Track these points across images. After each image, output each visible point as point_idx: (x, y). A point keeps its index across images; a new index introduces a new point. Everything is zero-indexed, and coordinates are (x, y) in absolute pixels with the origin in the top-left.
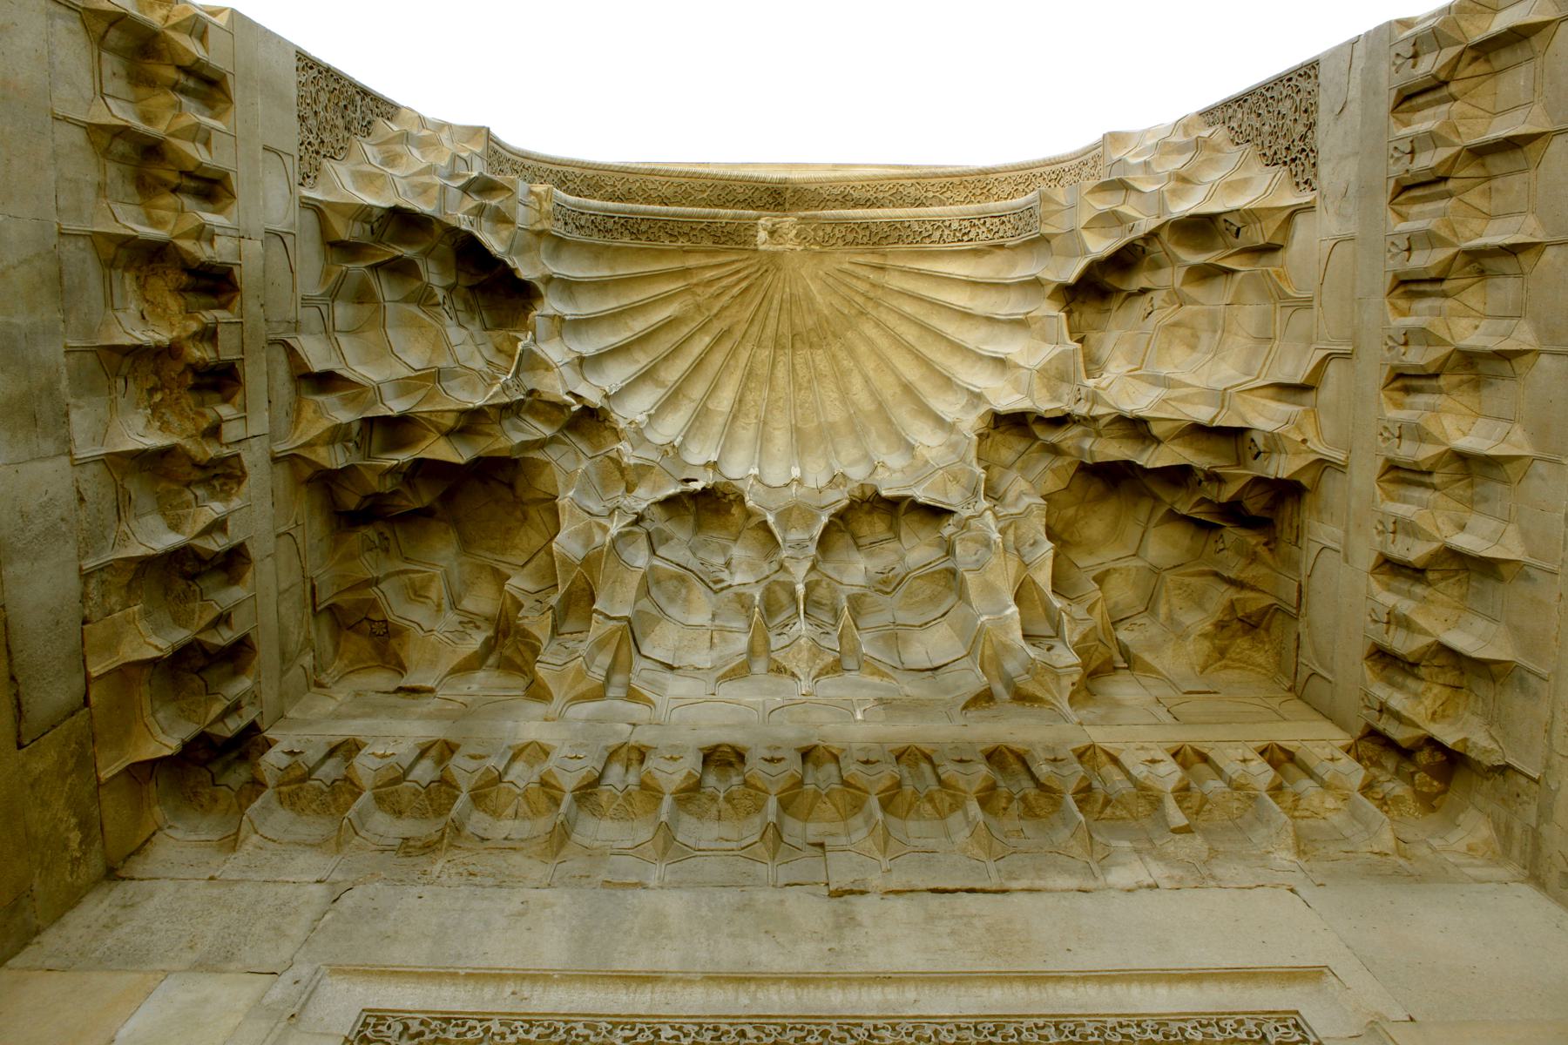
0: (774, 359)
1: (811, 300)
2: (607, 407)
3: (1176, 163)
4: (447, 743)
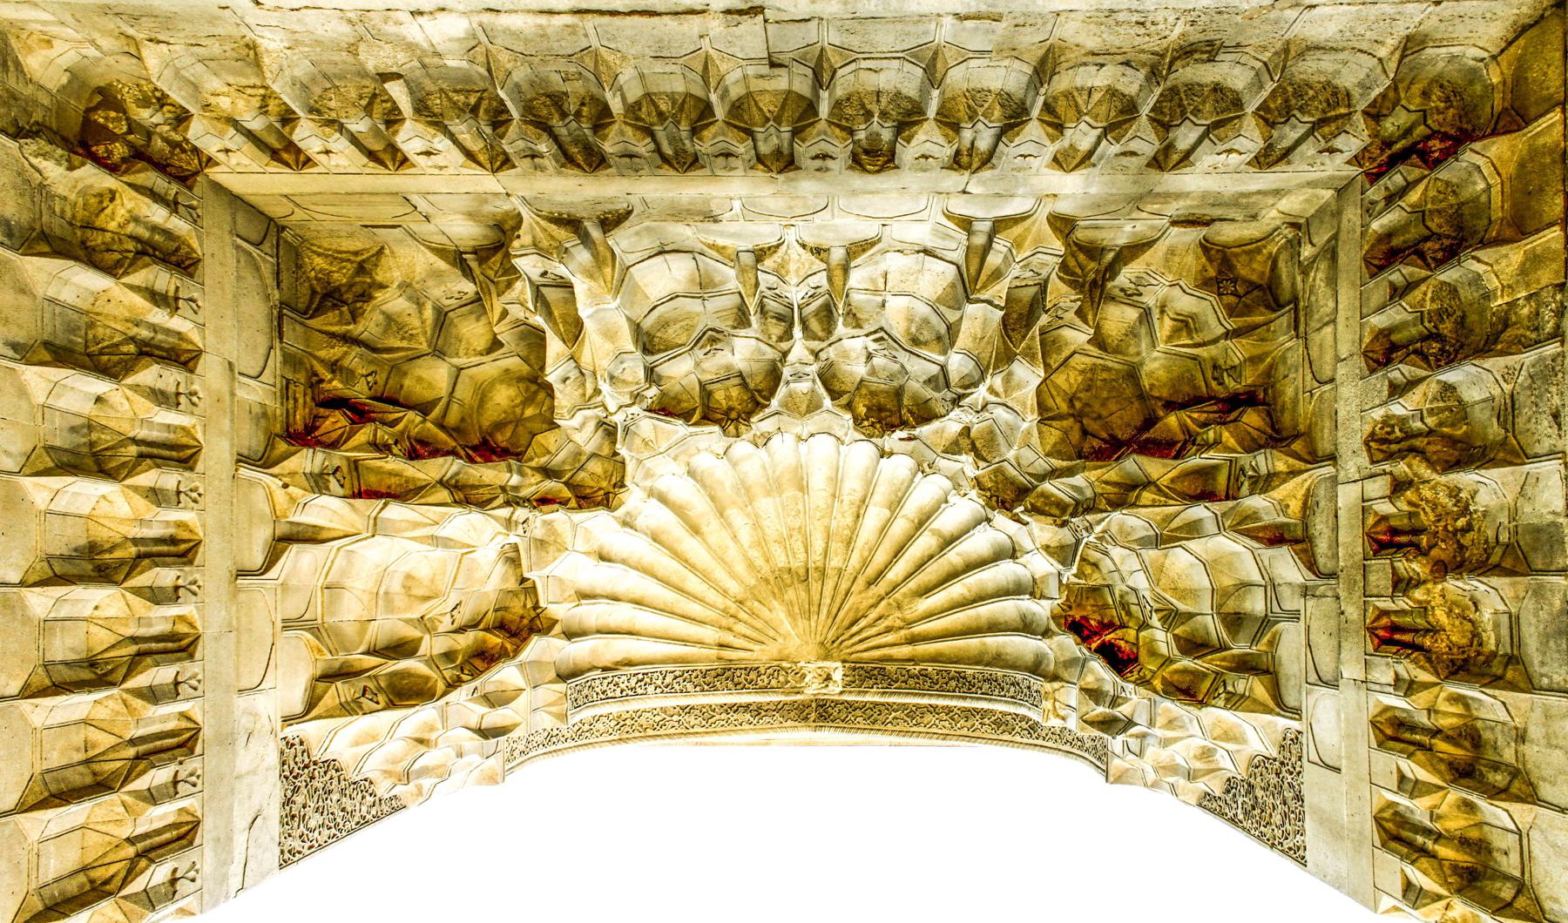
0: (825, 557)
1: (790, 614)
2: (988, 510)
3: (431, 758)
4: (1161, 169)
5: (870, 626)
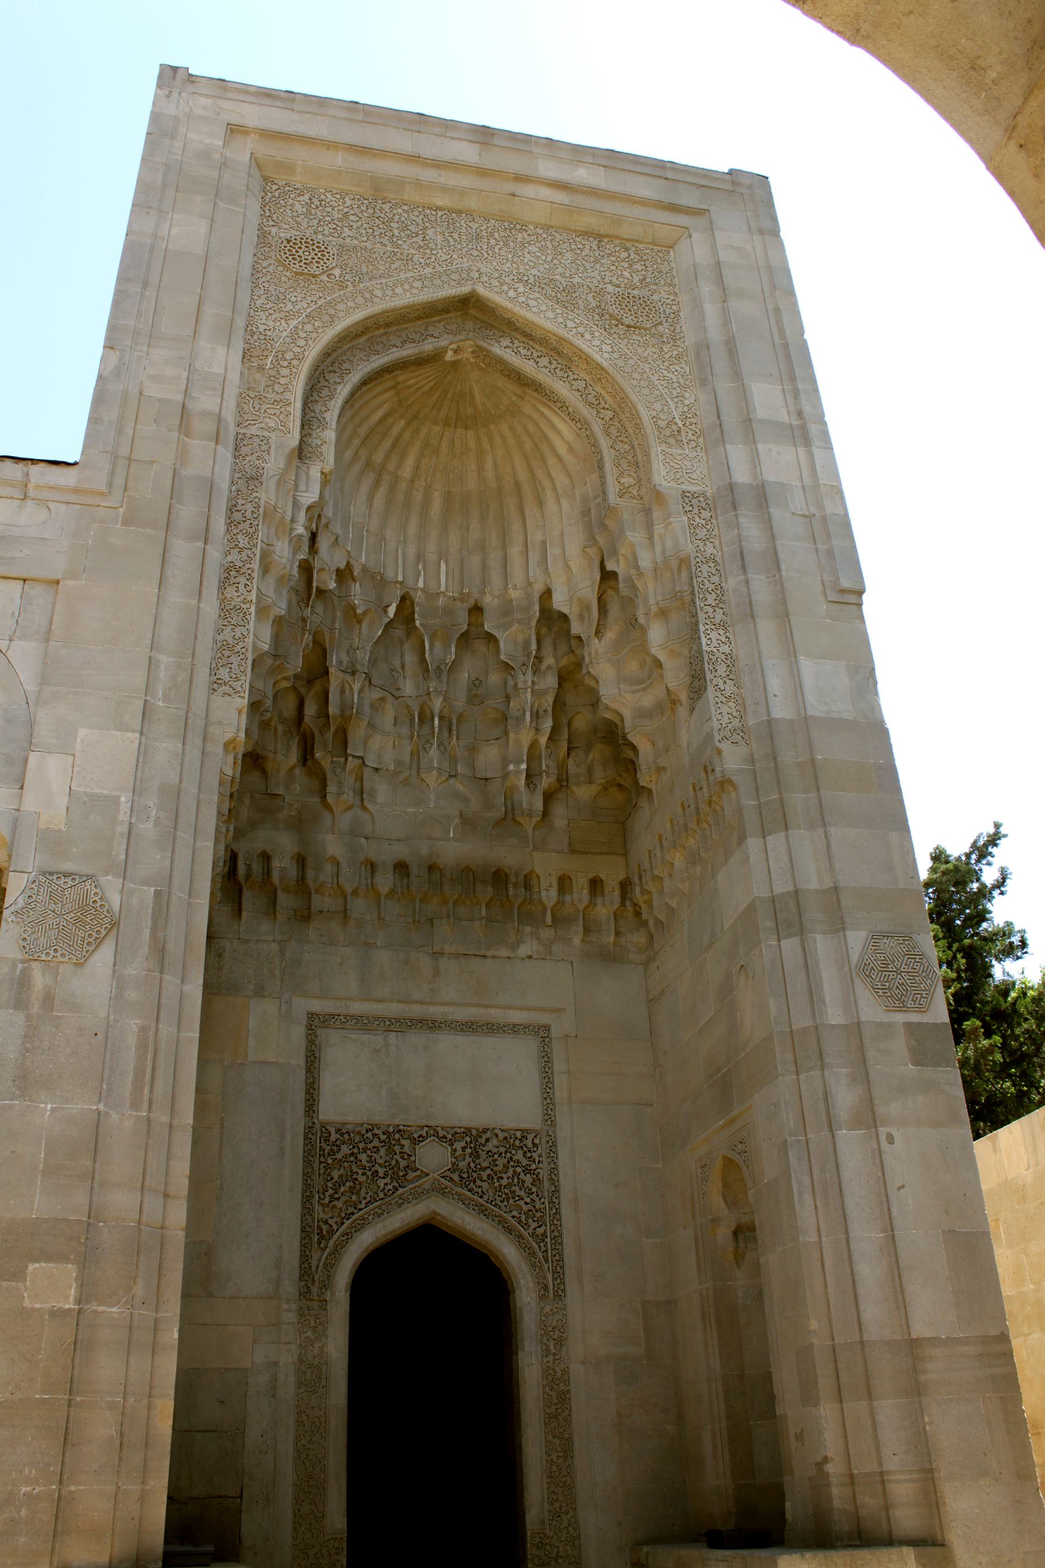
1: (472, 396)
5: (422, 387)
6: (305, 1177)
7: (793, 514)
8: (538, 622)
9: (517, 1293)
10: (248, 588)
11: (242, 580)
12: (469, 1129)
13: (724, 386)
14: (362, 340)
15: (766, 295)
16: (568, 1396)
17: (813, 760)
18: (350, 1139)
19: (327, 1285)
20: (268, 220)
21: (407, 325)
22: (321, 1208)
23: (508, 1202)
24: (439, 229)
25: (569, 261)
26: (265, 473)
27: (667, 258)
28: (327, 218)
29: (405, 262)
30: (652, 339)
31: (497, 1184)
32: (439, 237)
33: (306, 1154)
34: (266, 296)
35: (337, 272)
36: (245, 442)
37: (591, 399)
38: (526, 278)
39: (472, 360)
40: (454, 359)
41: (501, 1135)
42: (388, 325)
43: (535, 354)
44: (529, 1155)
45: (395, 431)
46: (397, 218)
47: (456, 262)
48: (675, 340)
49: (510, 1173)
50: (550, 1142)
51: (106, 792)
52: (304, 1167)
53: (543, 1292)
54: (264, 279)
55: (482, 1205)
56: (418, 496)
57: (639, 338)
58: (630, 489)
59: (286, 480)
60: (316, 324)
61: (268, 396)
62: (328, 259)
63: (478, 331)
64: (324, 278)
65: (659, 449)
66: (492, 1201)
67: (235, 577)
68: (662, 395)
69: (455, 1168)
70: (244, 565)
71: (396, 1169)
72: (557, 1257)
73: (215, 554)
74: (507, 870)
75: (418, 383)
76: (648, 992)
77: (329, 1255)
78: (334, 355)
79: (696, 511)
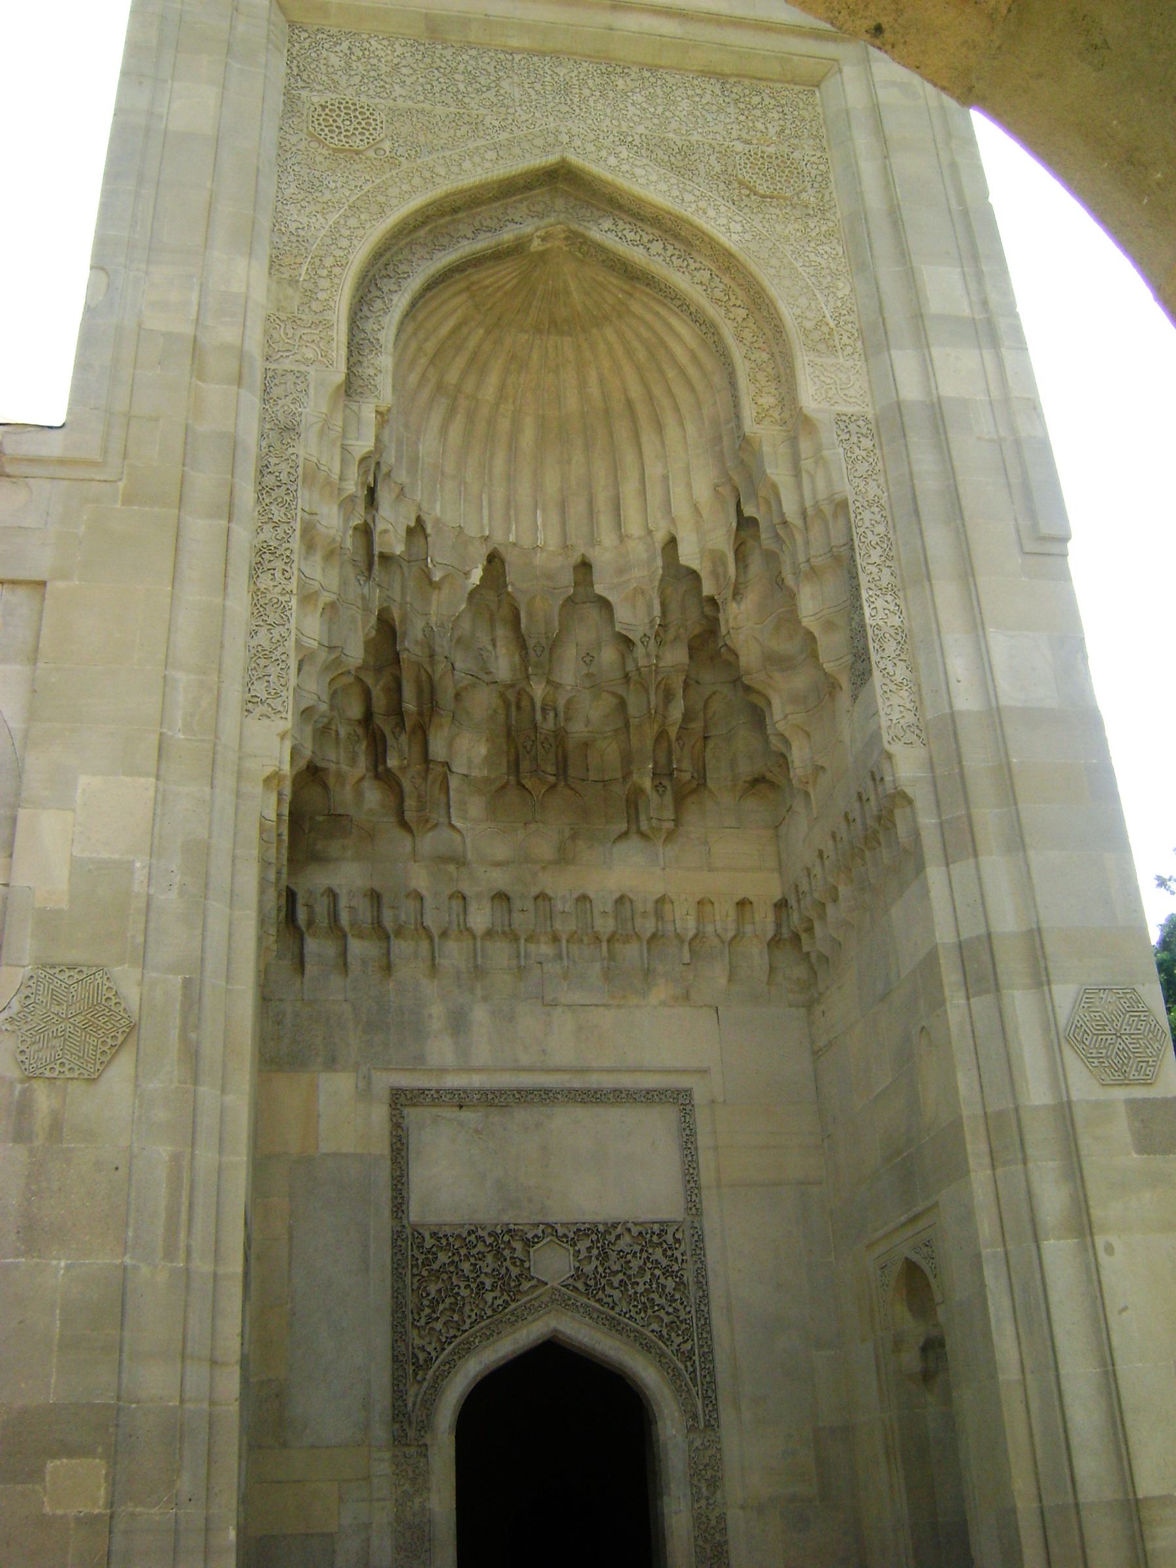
6: (395, 1294)
7: (979, 439)
8: (662, 580)
9: (660, 1424)
10: (287, 575)
11: (279, 564)
12: (596, 1225)
13: (887, 272)
14: (422, 233)
15: (940, 146)
16: (725, 1548)
17: (1009, 764)
18: (448, 1244)
19: (426, 1426)
20: (296, 81)
21: (479, 210)
22: (415, 1332)
23: (646, 1312)
24: (516, 78)
25: (685, 113)
26: (304, 421)
27: (811, 100)
28: (373, 74)
29: (474, 126)
30: (794, 211)
31: (631, 1292)
32: (517, 89)
33: (395, 1266)
34: (296, 183)
35: (387, 145)
36: (276, 381)
37: (718, 294)
38: (630, 139)
39: (565, 248)
40: (541, 248)
41: (635, 1232)
42: (455, 211)
43: (645, 239)
44: (669, 1253)
45: (472, 343)
46: (462, 67)
47: (539, 122)
48: (823, 212)
49: (647, 1278)
50: (696, 1236)
51: (117, 856)
52: (394, 1281)
53: (691, 1423)
54: (294, 160)
55: (614, 1319)
56: (504, 425)
57: (777, 211)
58: (771, 412)
59: (331, 426)
60: (363, 217)
61: (303, 317)
62: (375, 129)
63: (570, 211)
64: (371, 154)
65: (806, 358)
66: (626, 1313)
67: (270, 561)
68: (808, 287)
69: (579, 1274)
70: (281, 545)
71: (506, 1278)
72: (708, 1379)
73: (243, 535)
74: (631, 896)
75: (497, 282)
76: (813, 1042)
77: (428, 1388)
78: (388, 255)
79: (854, 439)
